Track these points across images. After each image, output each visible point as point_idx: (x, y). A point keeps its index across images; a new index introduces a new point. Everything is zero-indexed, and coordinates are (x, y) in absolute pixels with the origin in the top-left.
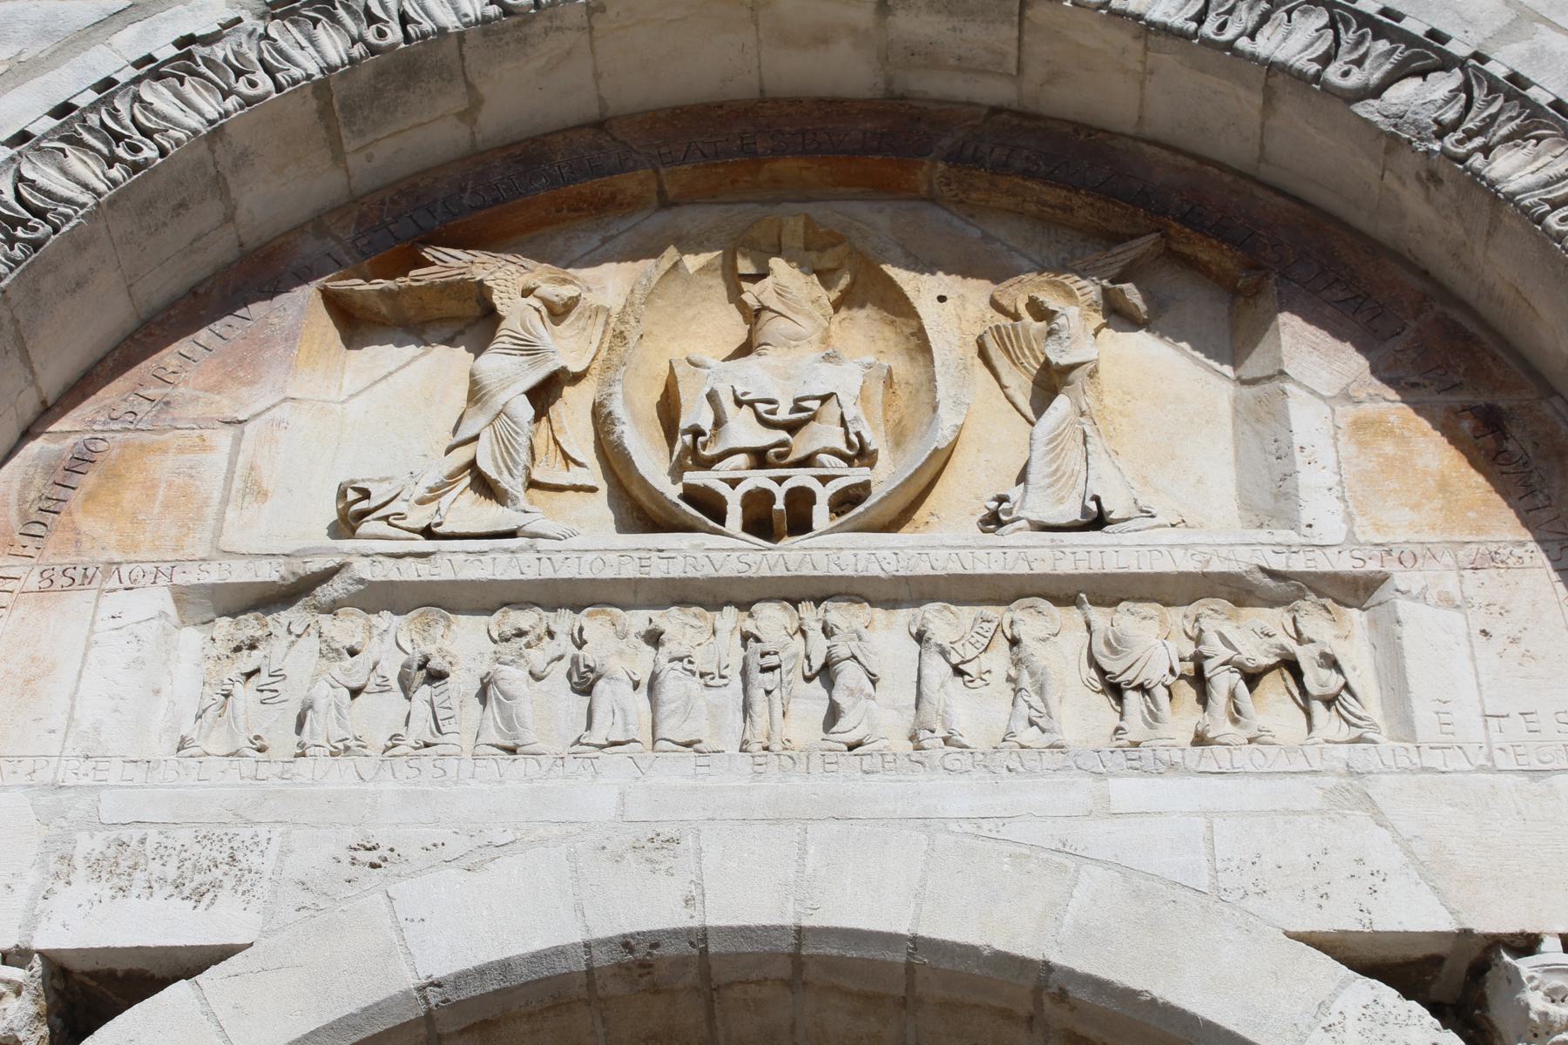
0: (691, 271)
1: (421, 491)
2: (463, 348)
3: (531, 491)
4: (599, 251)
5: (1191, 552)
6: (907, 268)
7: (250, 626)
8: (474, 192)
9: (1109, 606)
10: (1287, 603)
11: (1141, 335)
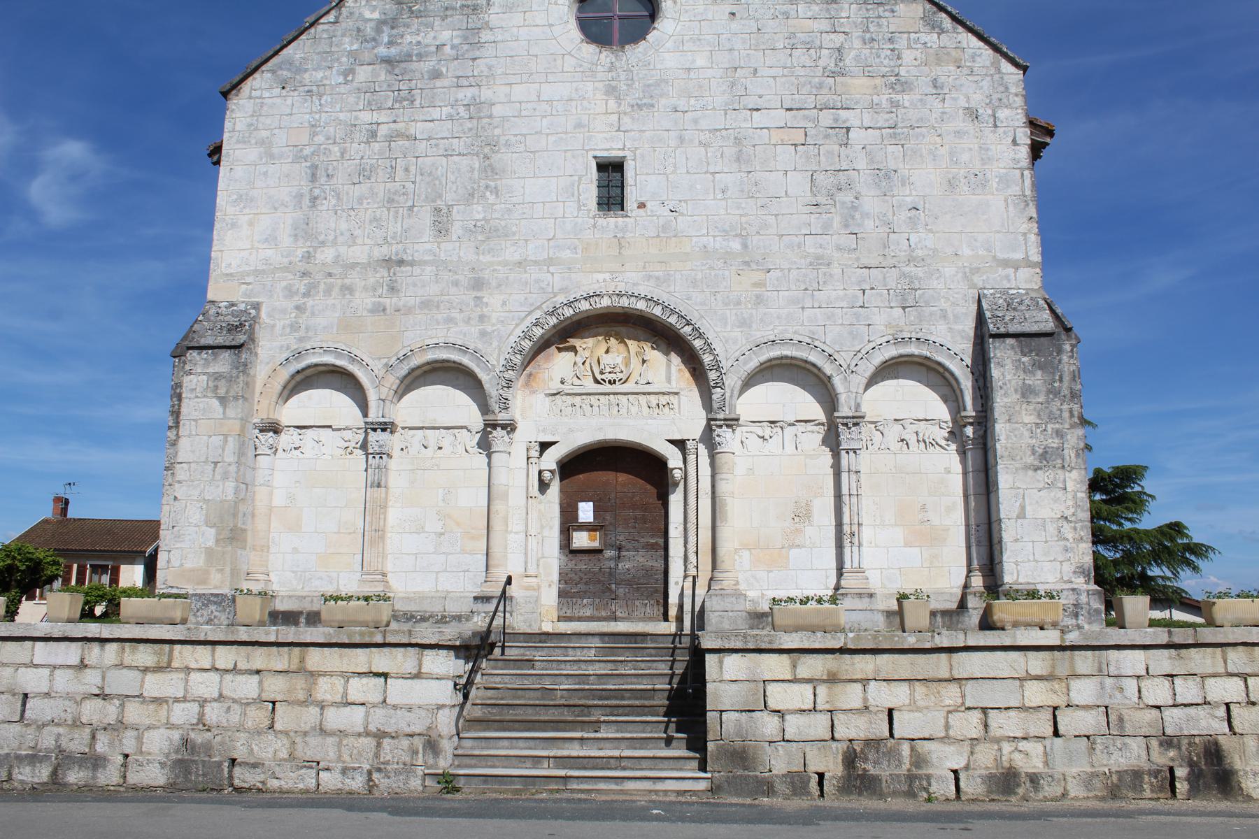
7: (553, 398)
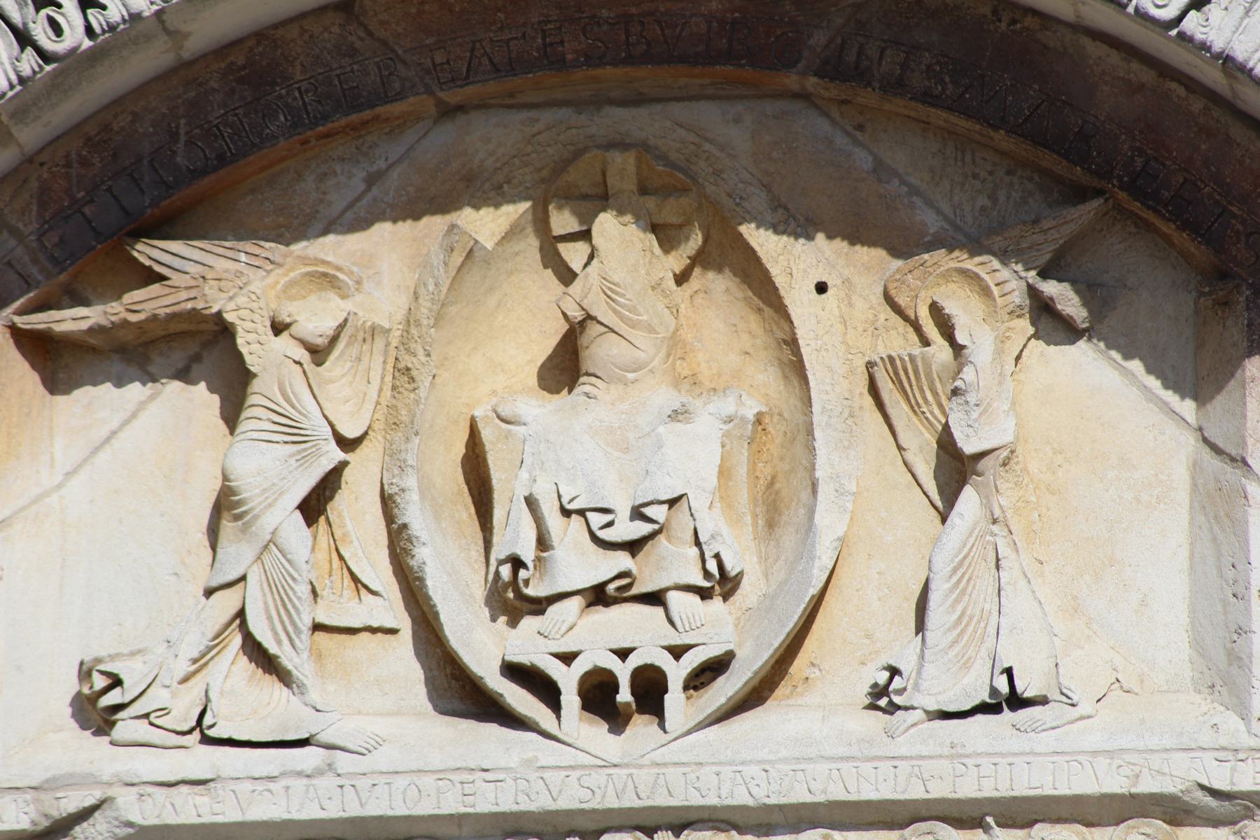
0: (489, 245)
1: (184, 667)
2: (202, 385)
3: (321, 636)
4: (364, 201)
5: (1117, 762)
6: (777, 229)
8: (190, 143)
9: (1022, 827)
10: (1234, 823)
11: (1083, 353)
